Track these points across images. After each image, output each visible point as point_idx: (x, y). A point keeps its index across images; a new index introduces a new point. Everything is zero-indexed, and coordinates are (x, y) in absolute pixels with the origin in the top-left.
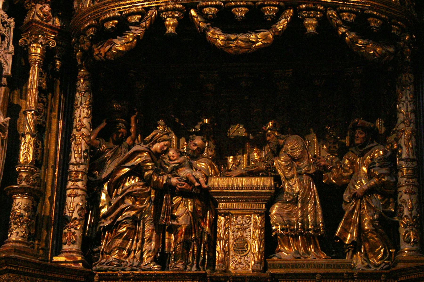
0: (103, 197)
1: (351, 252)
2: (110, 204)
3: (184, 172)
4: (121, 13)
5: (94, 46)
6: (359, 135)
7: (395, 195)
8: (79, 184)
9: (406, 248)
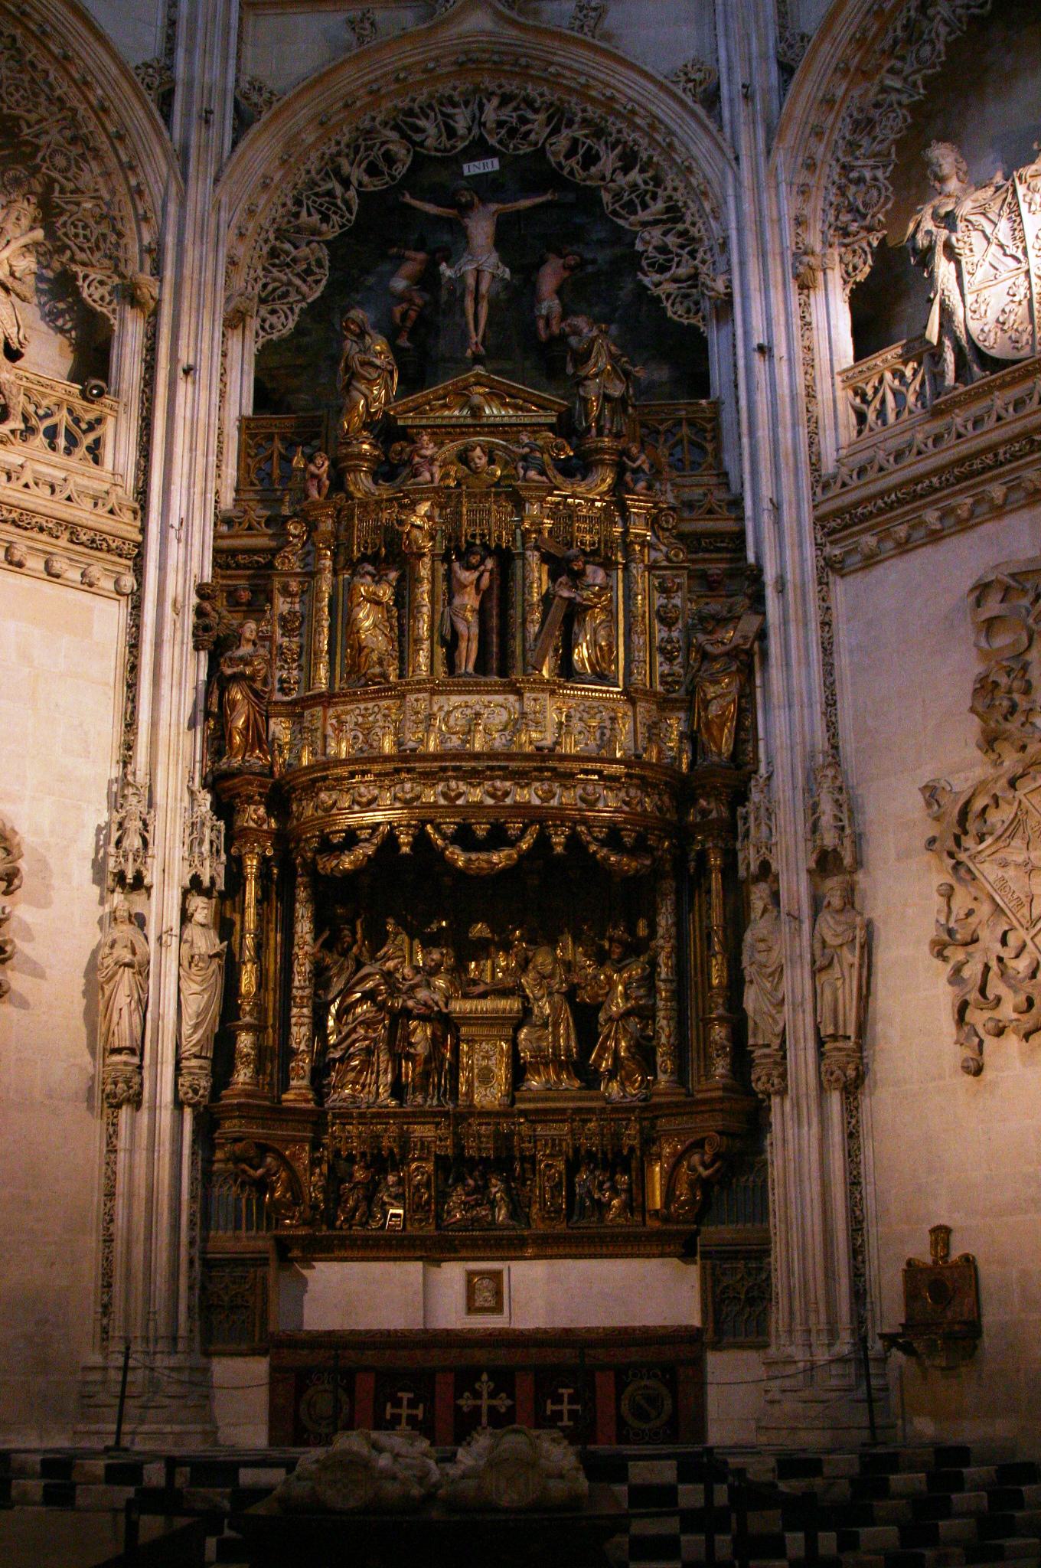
0: (331, 1023)
2: (340, 1032)
3: (422, 994)
7: (654, 1018)
8: (305, 1011)
9: (663, 1078)
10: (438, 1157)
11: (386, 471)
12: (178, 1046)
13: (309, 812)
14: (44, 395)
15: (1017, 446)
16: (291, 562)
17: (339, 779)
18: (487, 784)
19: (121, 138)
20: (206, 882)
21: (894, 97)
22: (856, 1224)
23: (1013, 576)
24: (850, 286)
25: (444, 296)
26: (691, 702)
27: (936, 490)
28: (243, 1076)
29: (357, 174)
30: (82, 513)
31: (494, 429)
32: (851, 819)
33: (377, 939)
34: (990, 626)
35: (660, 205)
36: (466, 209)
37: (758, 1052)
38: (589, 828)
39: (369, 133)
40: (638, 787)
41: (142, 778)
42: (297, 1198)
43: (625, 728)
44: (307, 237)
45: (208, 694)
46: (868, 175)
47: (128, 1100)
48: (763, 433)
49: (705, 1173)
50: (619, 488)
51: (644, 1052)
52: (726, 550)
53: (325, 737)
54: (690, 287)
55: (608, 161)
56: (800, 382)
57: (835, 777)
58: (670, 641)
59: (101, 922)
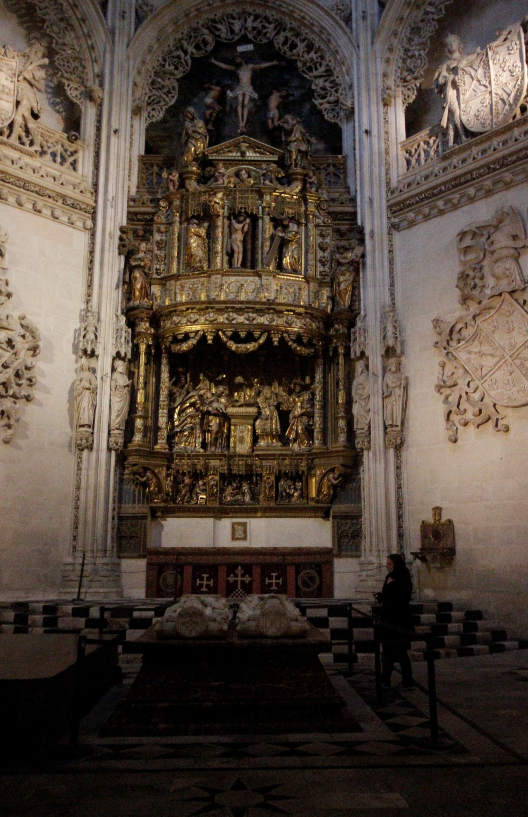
0: (176, 416)
3: (215, 405)
5: (172, 345)
7: (313, 417)
9: (317, 442)
10: (221, 474)
11: (203, 180)
12: (109, 425)
13: (168, 325)
14: (50, 137)
15: (482, 171)
16: (160, 218)
17: (182, 311)
18: (246, 315)
19: (84, 20)
20: (123, 354)
21: (431, 16)
22: (400, 506)
23: (477, 228)
24: (406, 105)
25: (228, 108)
26: (333, 283)
27: (443, 192)
28: (138, 438)
29: (191, 49)
30: (68, 191)
31: (251, 162)
32: (400, 335)
33: (196, 382)
34: (466, 250)
35: (322, 69)
36: (239, 66)
37: (358, 432)
38: (289, 335)
39: (196, 30)
40: (310, 318)
41: (95, 309)
42: (160, 490)
43: (305, 293)
44: (169, 76)
45: (124, 273)
46: (417, 53)
47: (87, 447)
48: (366, 168)
49: (335, 482)
50: (304, 190)
51: (309, 432)
52: (348, 220)
53: (175, 293)
54: (335, 106)
55: (301, 47)
56: (383, 146)
57: (394, 316)
58: (324, 257)
59: (76, 370)
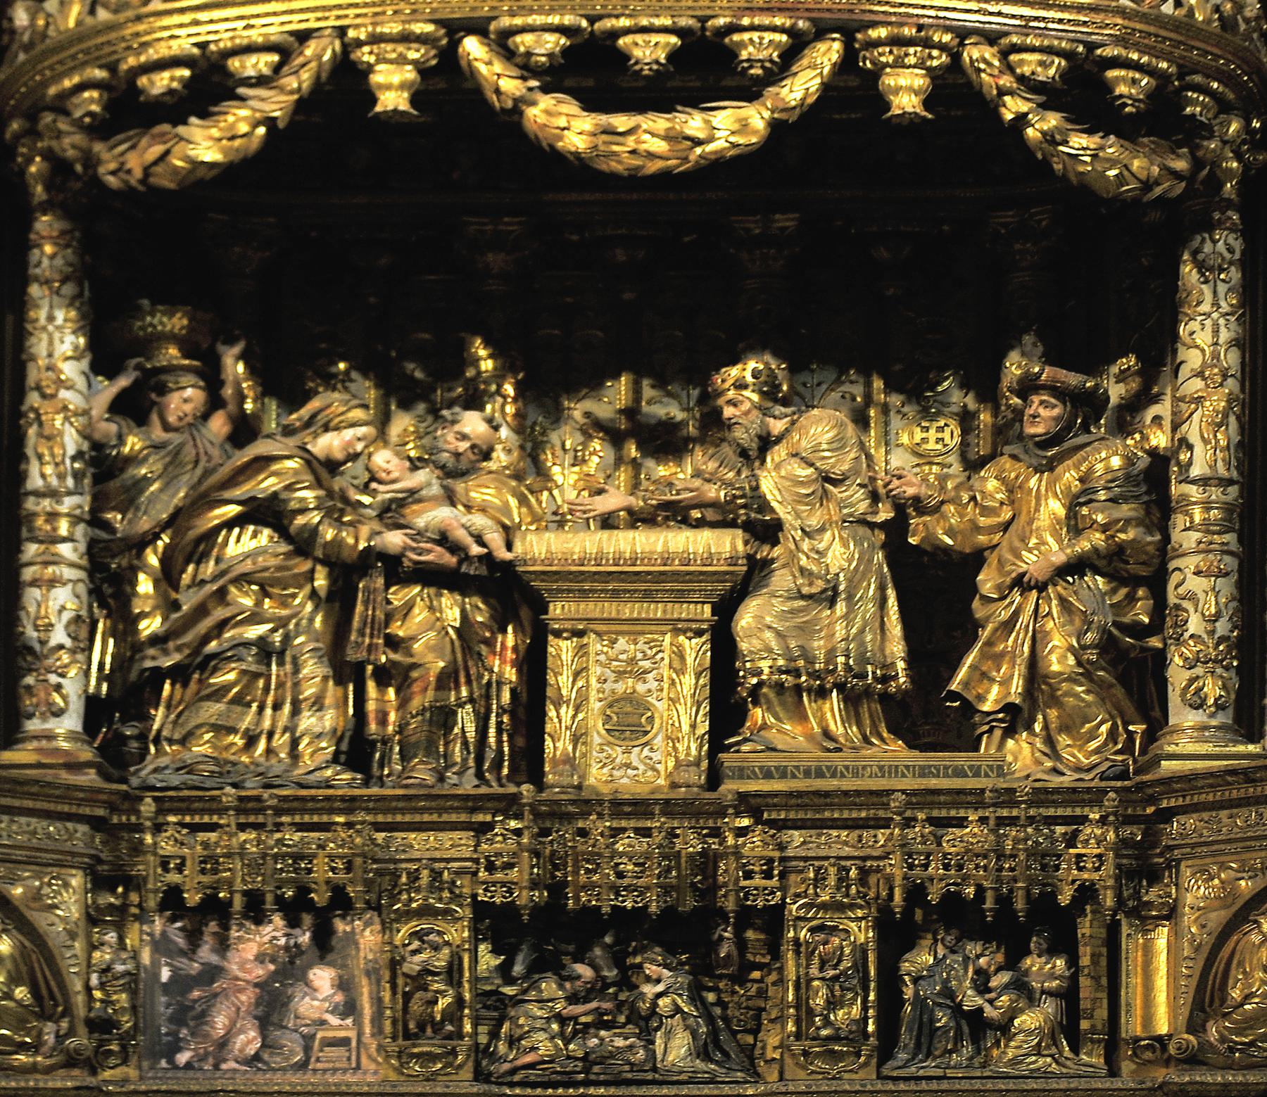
0: (145, 585)
1: (998, 733)
4: (203, 46)
6: (1041, 411)
